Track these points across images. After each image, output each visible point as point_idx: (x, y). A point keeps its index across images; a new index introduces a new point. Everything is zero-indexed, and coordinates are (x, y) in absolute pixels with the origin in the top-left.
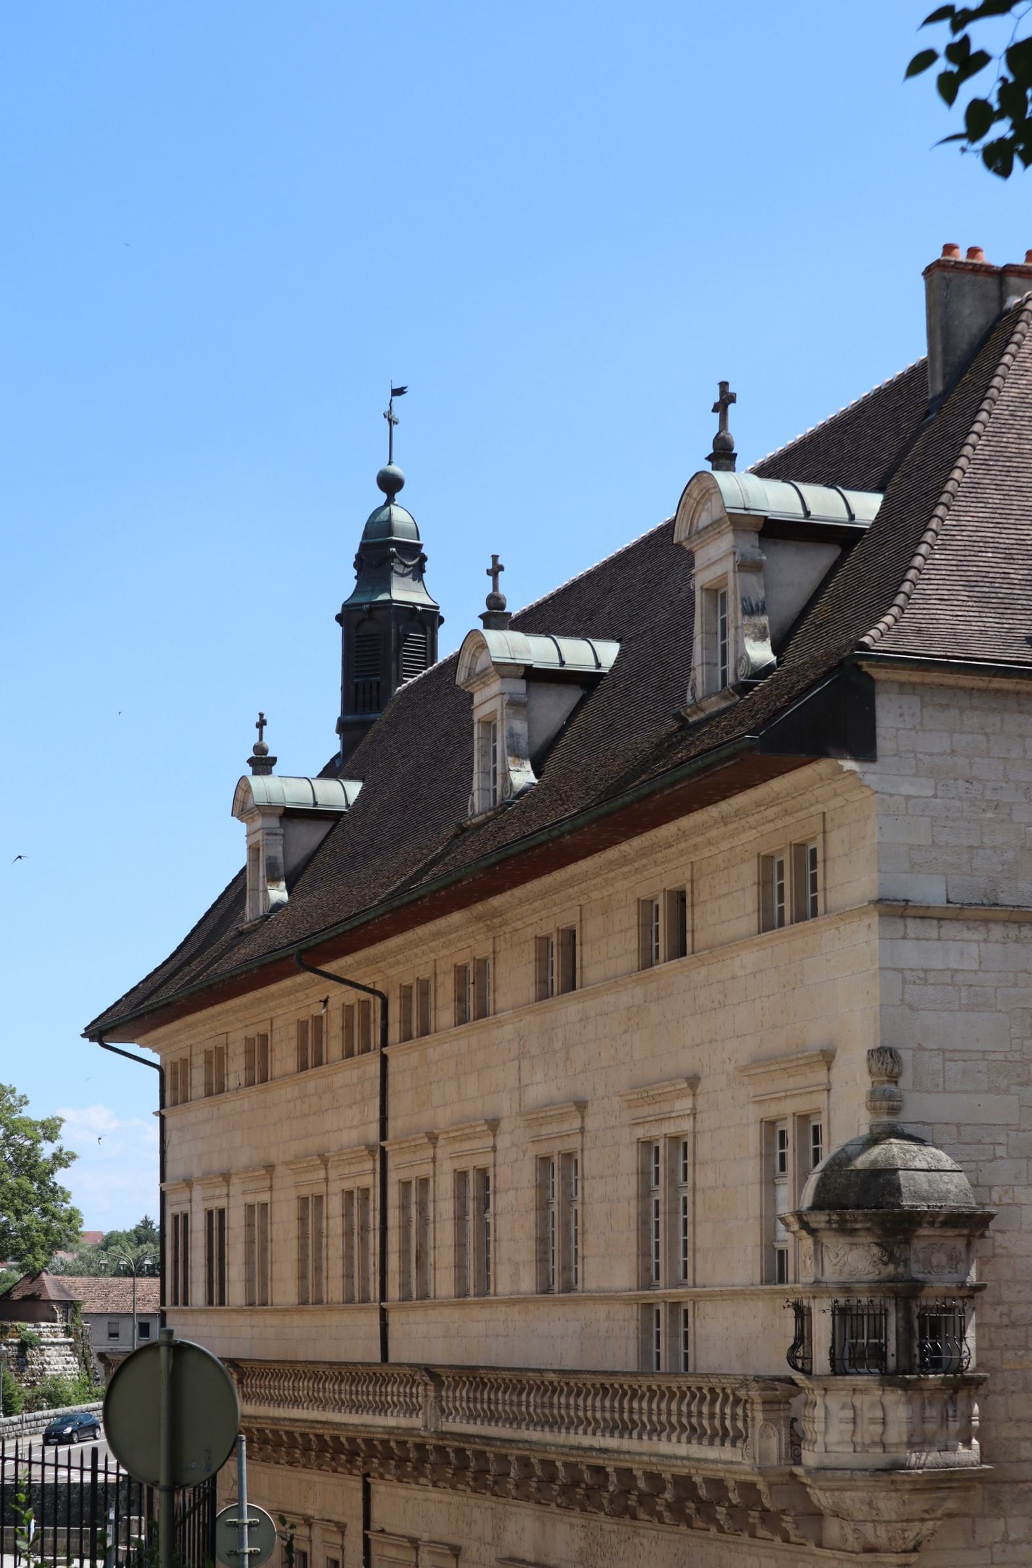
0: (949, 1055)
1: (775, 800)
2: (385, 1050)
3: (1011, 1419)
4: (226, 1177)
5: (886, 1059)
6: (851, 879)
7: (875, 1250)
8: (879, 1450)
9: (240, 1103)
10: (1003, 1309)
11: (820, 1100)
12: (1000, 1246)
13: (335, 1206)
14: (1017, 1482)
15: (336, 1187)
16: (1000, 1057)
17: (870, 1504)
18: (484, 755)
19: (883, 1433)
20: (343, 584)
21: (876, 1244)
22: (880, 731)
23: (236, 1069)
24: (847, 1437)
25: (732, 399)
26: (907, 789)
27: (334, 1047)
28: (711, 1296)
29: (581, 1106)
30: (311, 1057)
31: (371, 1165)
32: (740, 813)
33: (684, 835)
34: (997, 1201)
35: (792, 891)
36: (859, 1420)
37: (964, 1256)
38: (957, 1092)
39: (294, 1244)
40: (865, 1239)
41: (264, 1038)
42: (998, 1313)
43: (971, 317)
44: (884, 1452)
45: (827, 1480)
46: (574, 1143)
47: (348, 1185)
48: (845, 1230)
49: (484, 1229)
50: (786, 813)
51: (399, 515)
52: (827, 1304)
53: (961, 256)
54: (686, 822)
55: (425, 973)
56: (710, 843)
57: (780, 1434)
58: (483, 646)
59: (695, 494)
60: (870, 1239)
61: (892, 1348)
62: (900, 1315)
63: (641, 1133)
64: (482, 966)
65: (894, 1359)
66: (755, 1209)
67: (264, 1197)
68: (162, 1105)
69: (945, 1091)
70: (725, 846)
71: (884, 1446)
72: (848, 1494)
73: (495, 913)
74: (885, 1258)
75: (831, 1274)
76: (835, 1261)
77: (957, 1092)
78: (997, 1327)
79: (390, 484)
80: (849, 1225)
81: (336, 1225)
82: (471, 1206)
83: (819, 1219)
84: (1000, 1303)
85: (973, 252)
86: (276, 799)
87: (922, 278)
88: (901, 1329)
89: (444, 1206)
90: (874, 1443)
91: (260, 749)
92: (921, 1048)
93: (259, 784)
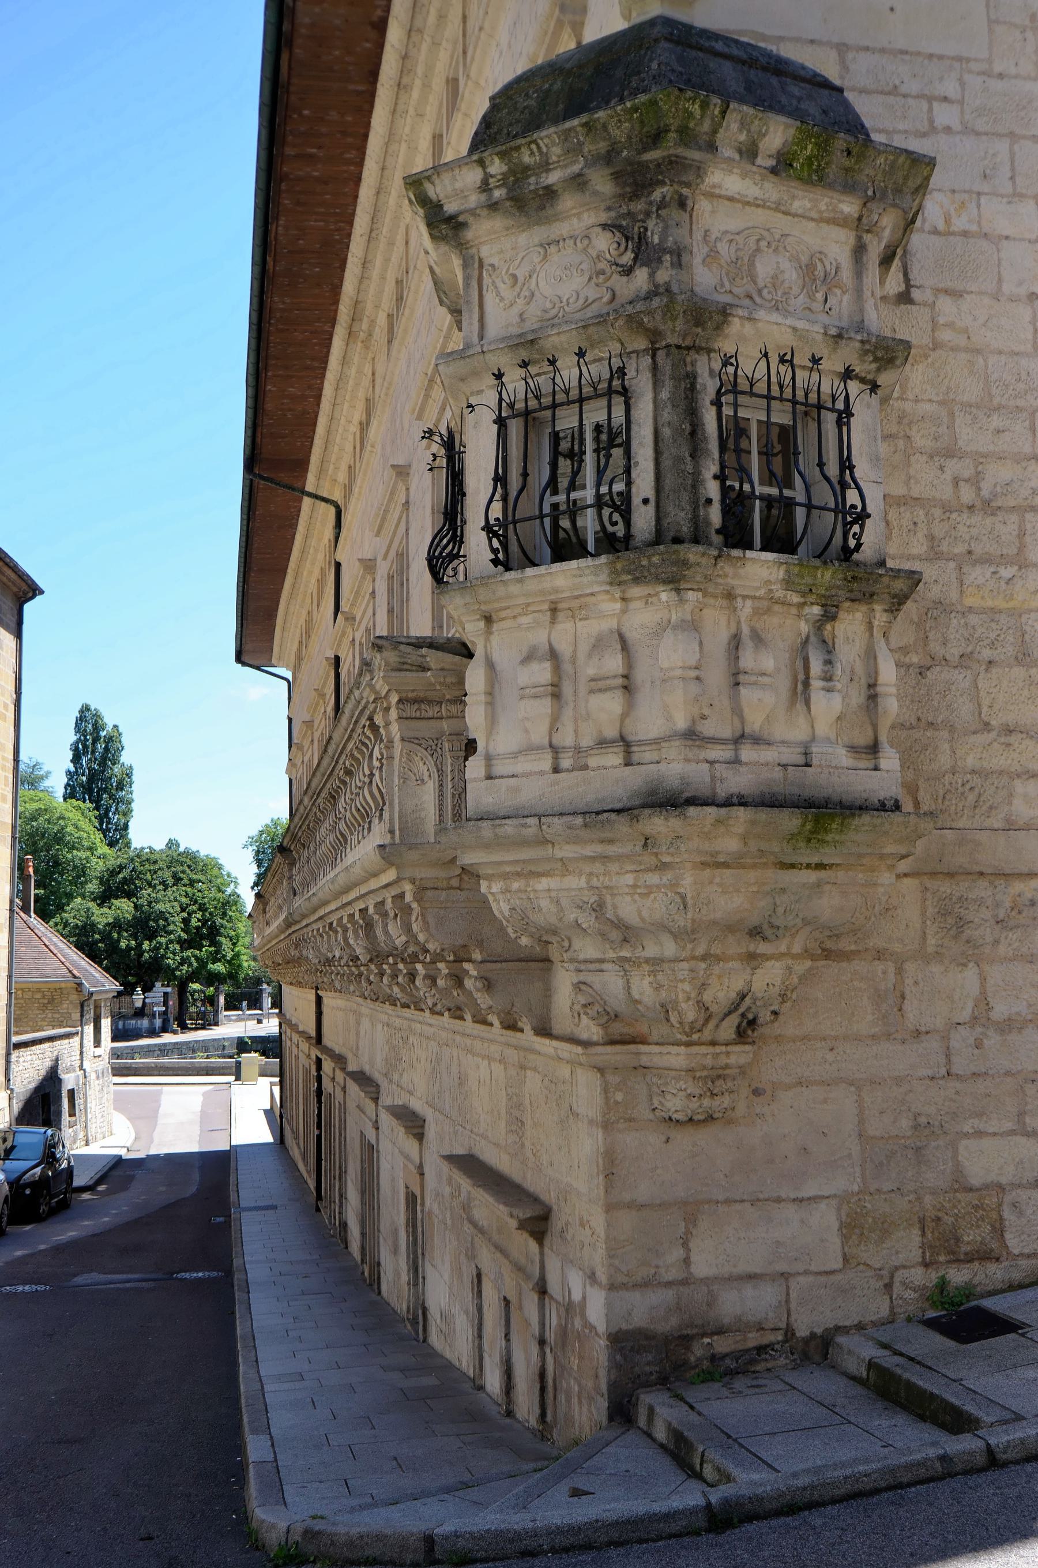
3: (987, 726)
7: (604, 243)
8: (614, 758)
14: (1008, 876)
17: (598, 908)
19: (624, 716)
21: (605, 226)
24: (539, 734)
34: (941, 226)
36: (567, 689)
37: (846, 275)
42: (948, 476)
45: (487, 846)
57: (441, 772)
60: (590, 218)
61: (644, 484)
62: (664, 395)
65: (651, 509)
72: (544, 883)
74: (628, 258)
78: (947, 509)
84: (951, 452)
90: (603, 743)
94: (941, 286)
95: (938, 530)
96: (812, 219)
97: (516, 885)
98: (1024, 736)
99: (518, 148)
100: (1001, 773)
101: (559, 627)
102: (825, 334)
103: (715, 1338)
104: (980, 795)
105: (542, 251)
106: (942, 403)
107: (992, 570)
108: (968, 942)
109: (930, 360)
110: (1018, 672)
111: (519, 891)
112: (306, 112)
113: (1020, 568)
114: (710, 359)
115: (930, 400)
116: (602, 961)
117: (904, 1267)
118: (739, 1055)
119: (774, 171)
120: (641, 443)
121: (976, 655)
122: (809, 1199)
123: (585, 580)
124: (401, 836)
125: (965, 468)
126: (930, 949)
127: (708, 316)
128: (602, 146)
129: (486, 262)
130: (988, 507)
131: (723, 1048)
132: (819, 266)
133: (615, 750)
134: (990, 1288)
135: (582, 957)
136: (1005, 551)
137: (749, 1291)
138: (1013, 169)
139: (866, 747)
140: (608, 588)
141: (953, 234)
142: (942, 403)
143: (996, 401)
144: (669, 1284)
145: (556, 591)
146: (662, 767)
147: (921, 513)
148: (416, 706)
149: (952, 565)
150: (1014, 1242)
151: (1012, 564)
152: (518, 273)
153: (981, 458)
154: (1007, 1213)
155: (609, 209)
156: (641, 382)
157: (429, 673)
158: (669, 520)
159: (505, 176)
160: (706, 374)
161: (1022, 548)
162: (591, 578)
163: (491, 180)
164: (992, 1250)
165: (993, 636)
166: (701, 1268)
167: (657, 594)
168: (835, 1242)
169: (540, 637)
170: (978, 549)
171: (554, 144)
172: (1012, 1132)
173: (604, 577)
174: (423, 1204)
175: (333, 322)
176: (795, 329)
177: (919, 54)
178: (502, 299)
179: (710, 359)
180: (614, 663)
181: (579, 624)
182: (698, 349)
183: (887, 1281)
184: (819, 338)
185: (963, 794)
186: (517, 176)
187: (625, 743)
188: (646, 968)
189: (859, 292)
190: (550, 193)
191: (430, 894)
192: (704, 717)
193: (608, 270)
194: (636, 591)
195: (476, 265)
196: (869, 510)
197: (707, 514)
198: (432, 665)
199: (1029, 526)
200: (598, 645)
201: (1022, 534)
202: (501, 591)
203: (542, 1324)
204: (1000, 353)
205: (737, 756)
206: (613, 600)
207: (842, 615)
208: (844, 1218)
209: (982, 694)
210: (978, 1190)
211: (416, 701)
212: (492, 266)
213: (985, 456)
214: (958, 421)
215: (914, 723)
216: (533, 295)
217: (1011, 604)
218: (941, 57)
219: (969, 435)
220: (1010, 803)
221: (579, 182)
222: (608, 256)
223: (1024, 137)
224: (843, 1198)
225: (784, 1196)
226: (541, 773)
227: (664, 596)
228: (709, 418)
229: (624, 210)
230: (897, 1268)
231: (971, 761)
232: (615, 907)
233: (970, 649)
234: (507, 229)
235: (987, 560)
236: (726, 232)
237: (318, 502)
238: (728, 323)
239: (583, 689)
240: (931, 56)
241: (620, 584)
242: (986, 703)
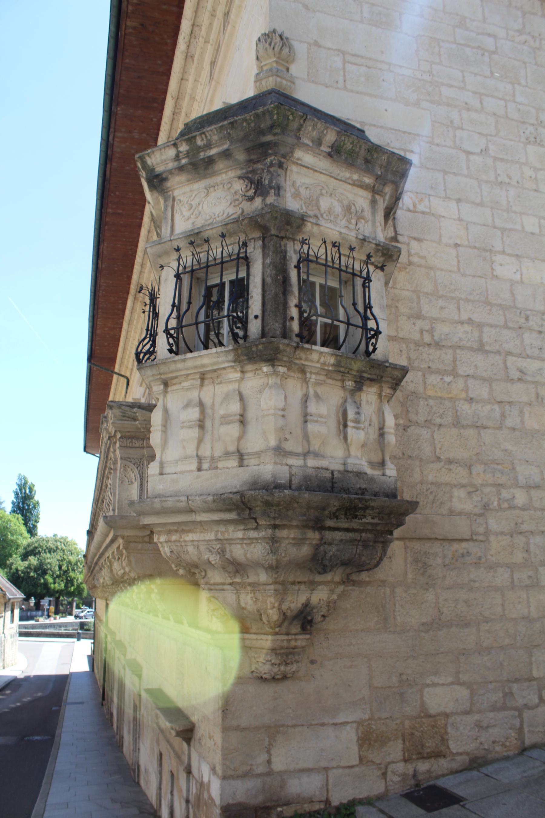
0: (348, 58)
3: (439, 459)
7: (239, 186)
8: (233, 463)
12: (417, 254)
19: (240, 438)
21: (240, 178)
24: (191, 450)
34: (411, 208)
36: (208, 423)
37: (367, 214)
42: (417, 328)
44: (241, 465)
60: (232, 174)
62: (268, 261)
65: (259, 321)
69: (345, 88)
71: (241, 457)
72: (190, 537)
74: (251, 193)
76: (187, 214)
80: (202, 155)
84: (419, 316)
88: (269, 280)
90: (227, 454)
92: (317, 44)
94: (412, 235)
95: (413, 356)
96: (349, 184)
97: (174, 538)
98: (458, 465)
99: (194, 137)
100: (446, 484)
101: (205, 388)
102: (357, 238)
103: (285, 807)
104: (435, 496)
105: (206, 191)
106: (414, 291)
107: (440, 377)
108: (429, 577)
109: (407, 270)
110: (454, 431)
111: (175, 541)
112: (117, 193)
113: (454, 377)
114: (294, 244)
115: (408, 290)
116: (223, 584)
117: (393, 762)
118: (301, 640)
119: (330, 155)
120: (255, 286)
121: (433, 421)
122: (341, 724)
123: (220, 360)
124: (118, 512)
126: (409, 581)
128: (241, 134)
129: (177, 198)
130: (438, 345)
131: (293, 637)
132: (353, 207)
133: (234, 457)
134: (440, 773)
135: (212, 582)
136: (447, 368)
137: (305, 779)
138: (445, 186)
139: (379, 463)
140: (233, 364)
141: (417, 212)
142: (414, 291)
143: (441, 293)
144: (258, 776)
145: (203, 366)
146: (261, 467)
147: (404, 346)
148: (130, 440)
149: (420, 373)
150: (454, 747)
151: (450, 375)
152: (192, 203)
153: (433, 320)
154: (449, 729)
155: (242, 169)
156: (255, 252)
157: (137, 422)
158: (269, 327)
159: (188, 152)
160: (292, 252)
161: (455, 367)
162: (224, 358)
163: (180, 154)
164: (441, 751)
165: (441, 411)
166: (278, 765)
167: (261, 369)
168: (355, 748)
169: (194, 395)
170: (433, 366)
171: (214, 135)
172: (452, 683)
173: (231, 357)
174: (140, 710)
175: (128, 292)
176: (341, 233)
177: (399, 131)
178: (184, 216)
179: (294, 244)
180: (235, 407)
181: (217, 387)
182: (288, 239)
183: (383, 771)
184: (354, 239)
185: (426, 495)
186: (195, 150)
187: (241, 457)
188: (249, 588)
189: (374, 222)
190: (210, 161)
191: (132, 545)
192: (286, 440)
193: (241, 199)
194: (249, 367)
195: (171, 200)
196: (380, 329)
197: (291, 325)
198: (139, 418)
199: (458, 356)
200: (227, 397)
201: (455, 360)
202: (173, 367)
203: (188, 791)
204: (442, 270)
205: (305, 463)
206: (236, 371)
207: (365, 388)
208: (360, 734)
209: (436, 442)
210: (434, 716)
211: (131, 438)
212: (180, 200)
213: (436, 319)
214: (422, 301)
215: (401, 455)
216: (200, 213)
217: (450, 396)
218: (410, 133)
219: (429, 309)
220: (451, 501)
221: (226, 154)
222: (241, 192)
223: (450, 173)
224: (359, 723)
225: (326, 722)
226: (191, 471)
227: (265, 369)
228: (293, 274)
229: (250, 169)
230: (389, 763)
231: (431, 478)
232: (231, 551)
233: (429, 418)
234: (188, 181)
235: (438, 372)
236: (304, 183)
237: (120, 377)
238: (305, 225)
239: (217, 422)
240: (404, 132)
241: (240, 362)
242: (438, 446)
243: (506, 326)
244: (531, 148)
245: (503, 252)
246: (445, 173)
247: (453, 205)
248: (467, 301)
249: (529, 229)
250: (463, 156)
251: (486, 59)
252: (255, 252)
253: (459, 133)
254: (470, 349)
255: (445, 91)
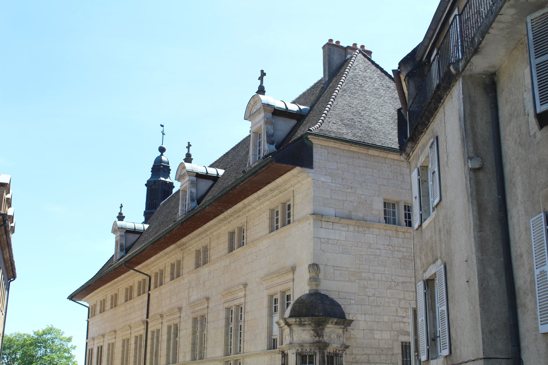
0: (336, 268)
1: (277, 187)
2: (150, 292)
4: (103, 336)
5: (314, 267)
6: (302, 208)
7: (312, 332)
9: (109, 313)
10: (353, 356)
11: (290, 285)
13: (132, 341)
15: (133, 335)
16: (352, 270)
18: (183, 200)
20: (148, 175)
22: (314, 160)
23: (108, 304)
25: (265, 74)
26: (323, 179)
27: (135, 293)
28: (249, 356)
29: (208, 299)
30: (129, 297)
31: (143, 327)
32: (265, 195)
33: (245, 206)
35: (282, 218)
37: (342, 336)
38: (338, 281)
39: (121, 353)
40: (308, 328)
41: (116, 295)
43: (337, 60)
46: (205, 312)
47: (137, 334)
48: (301, 324)
49: (176, 343)
50: (281, 192)
51: (164, 158)
52: (294, 351)
53: (334, 42)
54: (246, 201)
55: (162, 268)
56: (254, 208)
58: (184, 167)
59: (252, 103)
60: (310, 328)
63: (226, 305)
64: (179, 263)
66: (265, 325)
67: (113, 341)
68: (88, 318)
69: (334, 280)
70: (258, 208)
73: (184, 244)
75: (296, 339)
77: (338, 281)
79: (162, 150)
80: (303, 323)
81: (132, 347)
82: (172, 336)
83: (292, 320)
84: (352, 354)
85: (338, 42)
86: (124, 226)
87: (322, 50)
89: (164, 337)
91: (120, 214)
92: (326, 265)
93: (120, 223)
125: (353, 356)
127: (326, 345)
153: (356, 355)
219: (355, 352)
243: (376, 354)
244: (389, 291)
245: (377, 330)
246: (362, 305)
247: (363, 316)
248: (366, 347)
249: (385, 321)
250: (367, 298)
251: (377, 259)
252: (318, 353)
253: (367, 290)
254: (366, 363)
255: (364, 275)
